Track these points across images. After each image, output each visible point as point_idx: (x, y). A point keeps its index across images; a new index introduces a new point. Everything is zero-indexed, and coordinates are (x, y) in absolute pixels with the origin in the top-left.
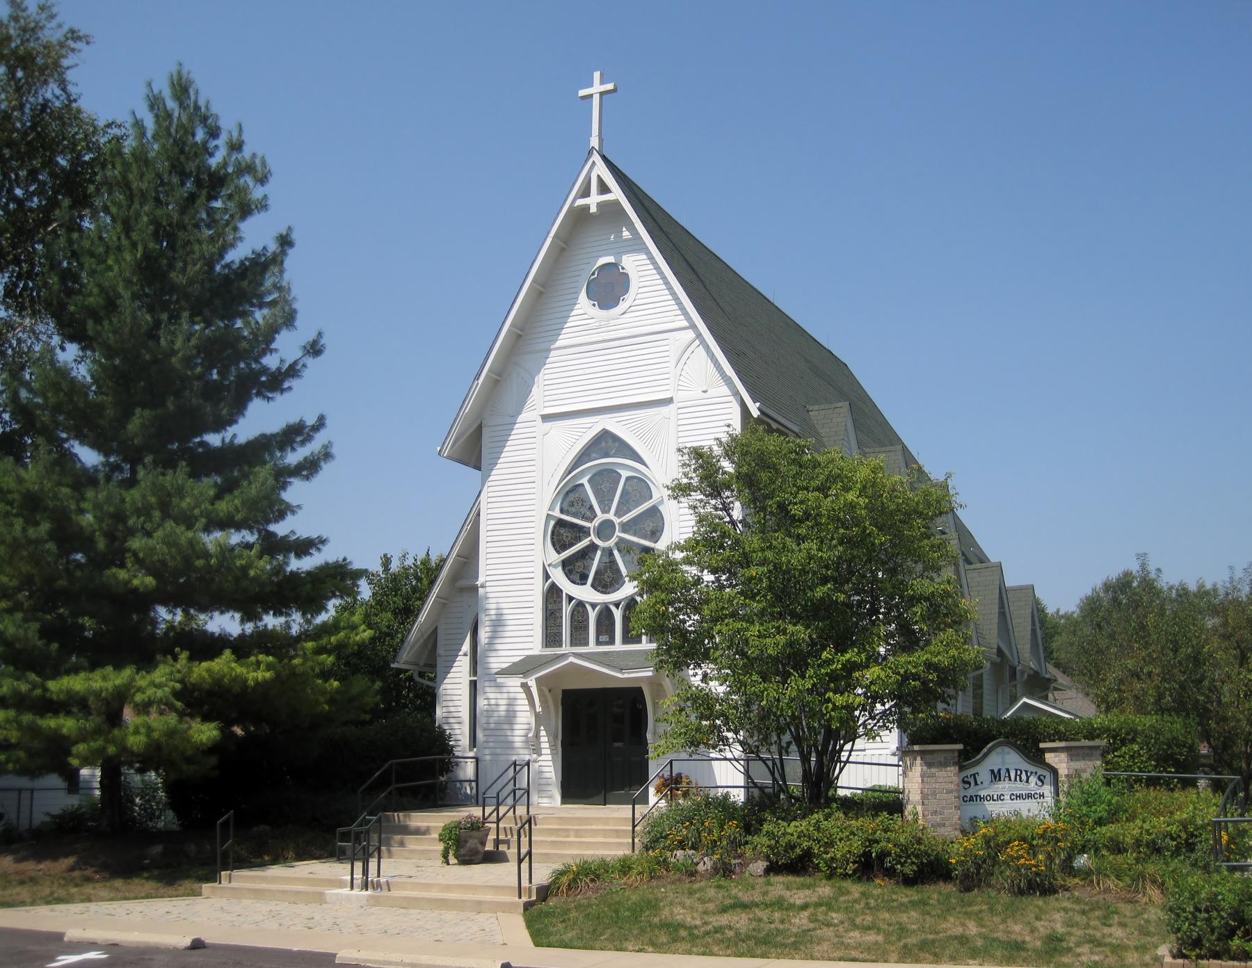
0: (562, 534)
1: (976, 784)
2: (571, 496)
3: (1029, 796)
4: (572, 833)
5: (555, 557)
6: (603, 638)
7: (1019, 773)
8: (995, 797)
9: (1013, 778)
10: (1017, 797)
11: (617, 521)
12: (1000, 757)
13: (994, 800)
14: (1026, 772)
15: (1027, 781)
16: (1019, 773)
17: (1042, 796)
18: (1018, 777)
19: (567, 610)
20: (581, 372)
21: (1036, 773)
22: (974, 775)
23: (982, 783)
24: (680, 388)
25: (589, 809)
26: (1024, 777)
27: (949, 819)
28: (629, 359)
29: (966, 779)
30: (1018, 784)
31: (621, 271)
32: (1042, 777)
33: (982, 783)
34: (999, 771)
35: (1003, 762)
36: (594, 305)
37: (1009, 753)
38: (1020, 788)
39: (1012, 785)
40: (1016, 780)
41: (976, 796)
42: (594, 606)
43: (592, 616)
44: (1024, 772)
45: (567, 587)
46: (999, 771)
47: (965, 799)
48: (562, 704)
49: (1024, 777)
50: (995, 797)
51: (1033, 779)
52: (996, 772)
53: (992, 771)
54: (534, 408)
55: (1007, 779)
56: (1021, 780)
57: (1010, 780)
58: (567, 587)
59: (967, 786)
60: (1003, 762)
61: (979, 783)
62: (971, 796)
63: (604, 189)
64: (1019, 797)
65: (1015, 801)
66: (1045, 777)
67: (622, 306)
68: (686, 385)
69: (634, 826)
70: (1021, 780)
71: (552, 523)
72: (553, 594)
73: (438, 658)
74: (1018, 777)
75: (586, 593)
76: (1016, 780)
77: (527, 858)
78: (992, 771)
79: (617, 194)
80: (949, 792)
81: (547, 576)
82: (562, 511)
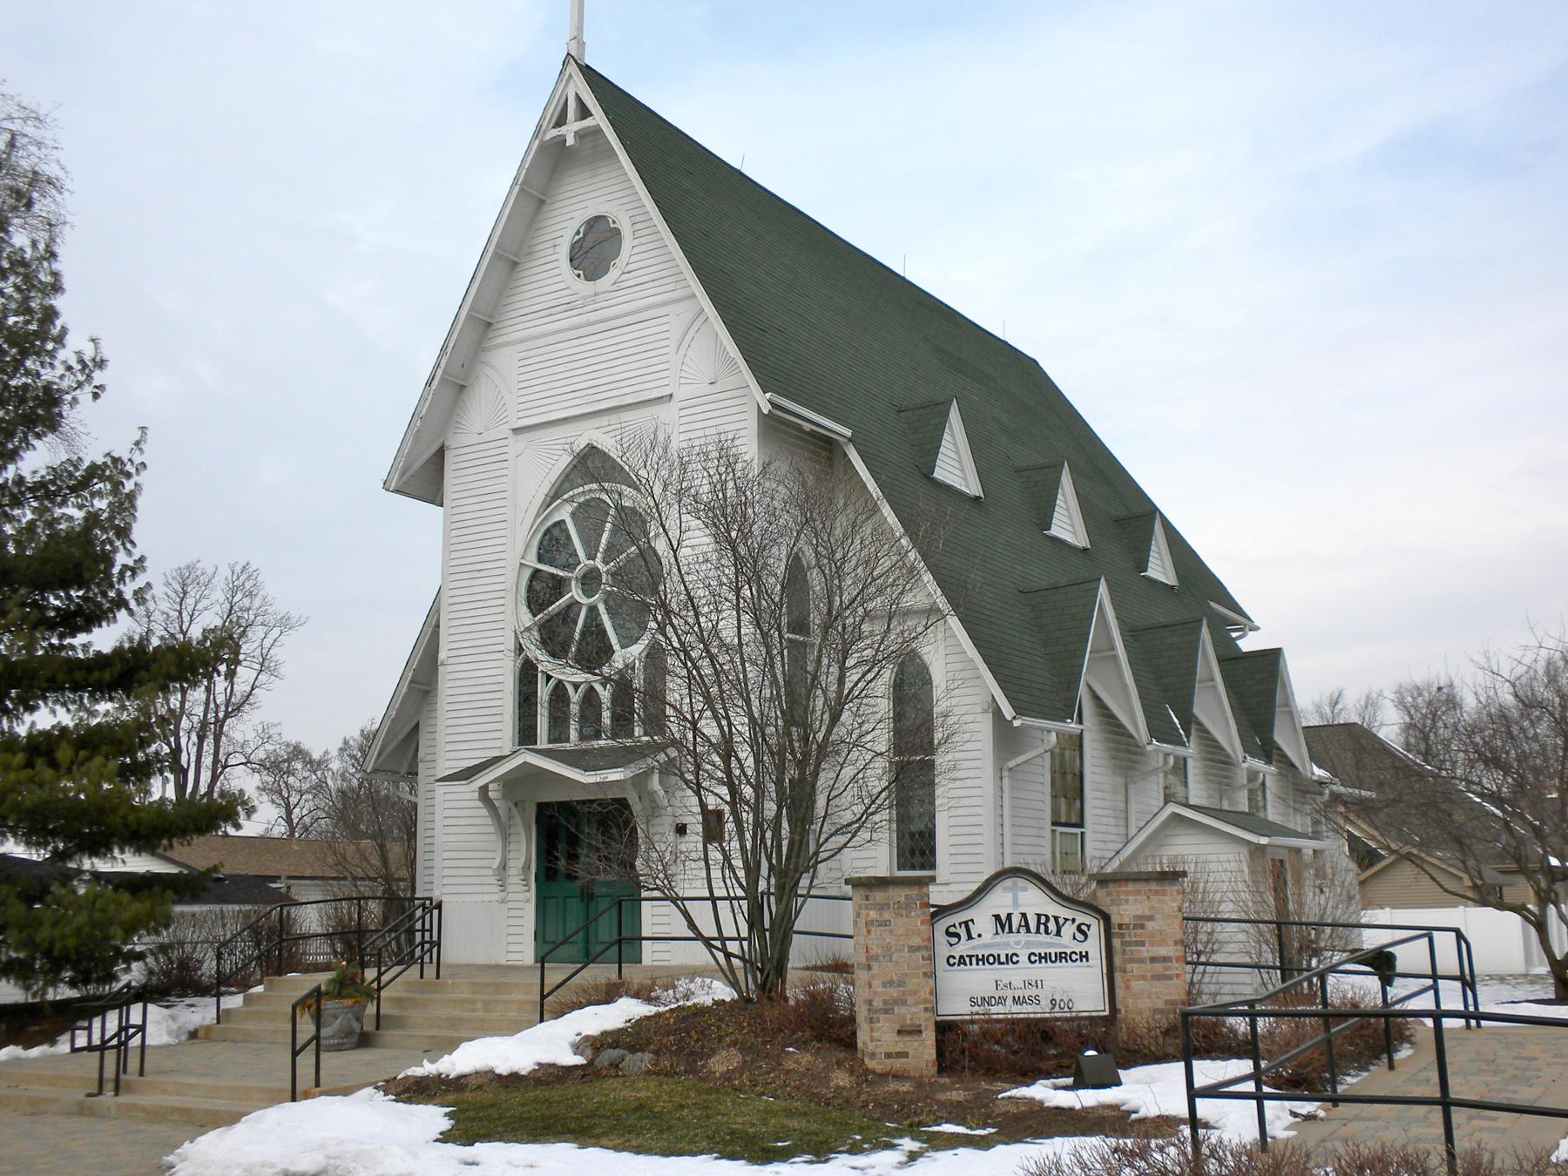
0: (541, 591)
1: (970, 937)
2: (552, 543)
3: (1062, 957)
4: (479, 1006)
5: (527, 619)
6: (588, 731)
7: (1043, 920)
8: (1003, 959)
9: (1033, 927)
10: (1041, 958)
11: (603, 568)
12: (1011, 895)
13: (1000, 963)
14: (1056, 918)
15: (1058, 933)
16: (1043, 920)
17: (1084, 956)
18: (1042, 927)
19: (543, 692)
20: (562, 368)
21: (1074, 920)
22: (966, 923)
23: (980, 936)
24: (682, 381)
25: (562, 968)
26: (1052, 926)
27: (914, 992)
28: (621, 346)
29: (952, 930)
30: (1042, 937)
31: (612, 226)
32: (1083, 927)
33: (980, 936)
34: (1009, 916)
35: (1016, 904)
36: (579, 276)
37: (1025, 889)
38: (1044, 943)
39: (1032, 937)
40: (1038, 931)
41: (970, 957)
42: (576, 686)
43: (575, 697)
44: (1052, 919)
45: (545, 662)
46: (1009, 916)
47: (952, 961)
48: (537, 823)
49: (1052, 926)
50: (1003, 959)
51: (1068, 930)
52: (1004, 919)
53: (997, 917)
54: (504, 421)
55: (1023, 930)
56: (1047, 932)
57: (1028, 931)
58: (545, 662)
59: (955, 940)
60: (1016, 904)
61: (974, 935)
62: (962, 957)
63: (584, 113)
64: (1045, 958)
65: (1037, 964)
66: (1089, 926)
67: (613, 274)
68: (692, 371)
69: (543, 997)
70: (1047, 932)
71: (527, 574)
72: (528, 674)
73: (420, 765)
74: (1042, 927)
75: (573, 676)
76: (1038, 931)
77: (300, 1043)
78: (997, 917)
79: (599, 118)
80: (913, 949)
81: (520, 649)
82: (540, 559)
